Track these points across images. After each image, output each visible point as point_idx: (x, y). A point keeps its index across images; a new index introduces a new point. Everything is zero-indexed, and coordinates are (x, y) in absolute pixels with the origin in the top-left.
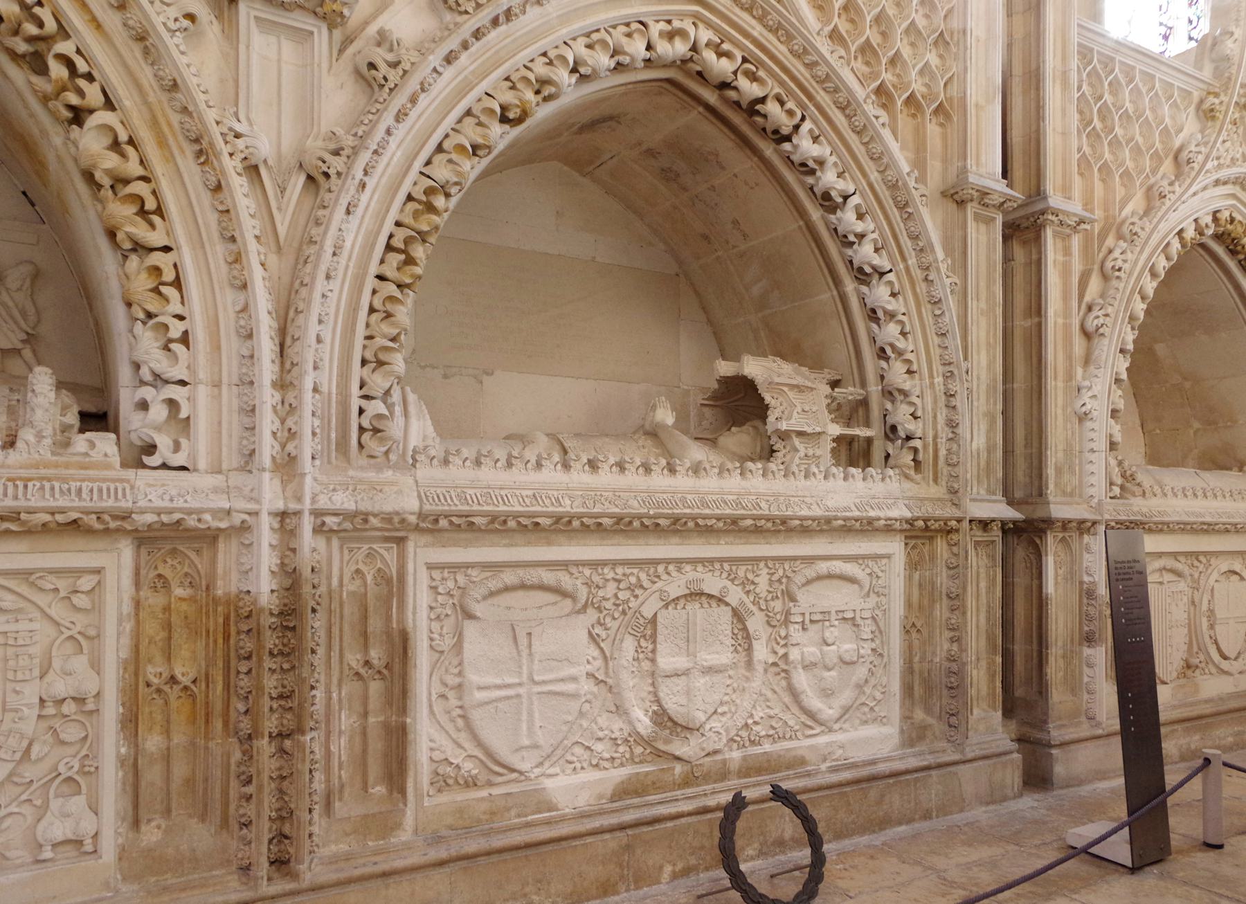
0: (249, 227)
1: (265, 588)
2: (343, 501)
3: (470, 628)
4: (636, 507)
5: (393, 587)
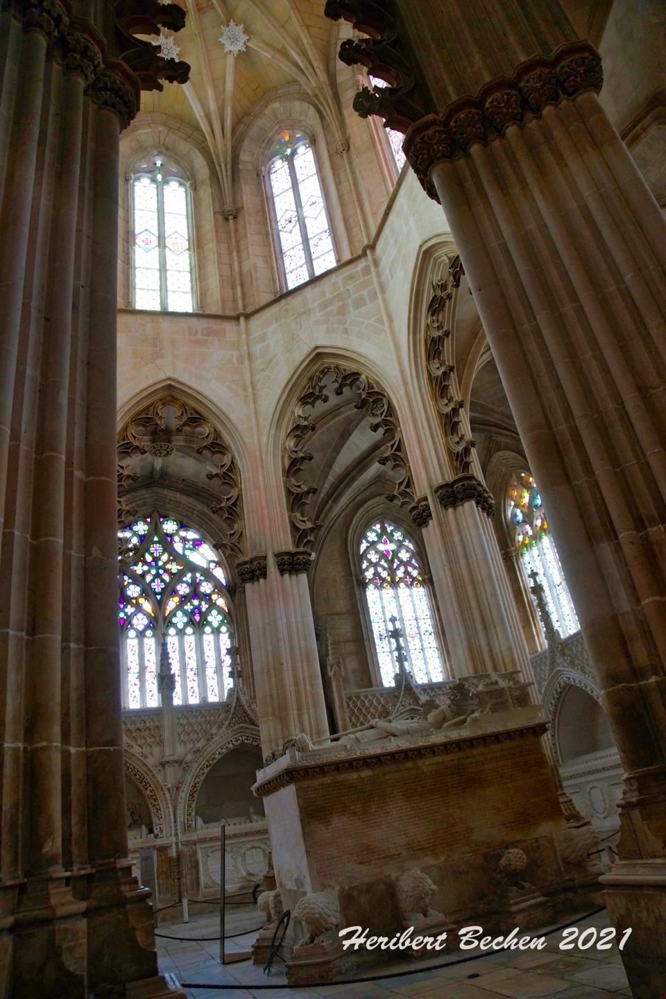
0: (169, 799)
1: (174, 854)
2: (185, 839)
3: (209, 859)
4: (237, 832)
5: (195, 853)
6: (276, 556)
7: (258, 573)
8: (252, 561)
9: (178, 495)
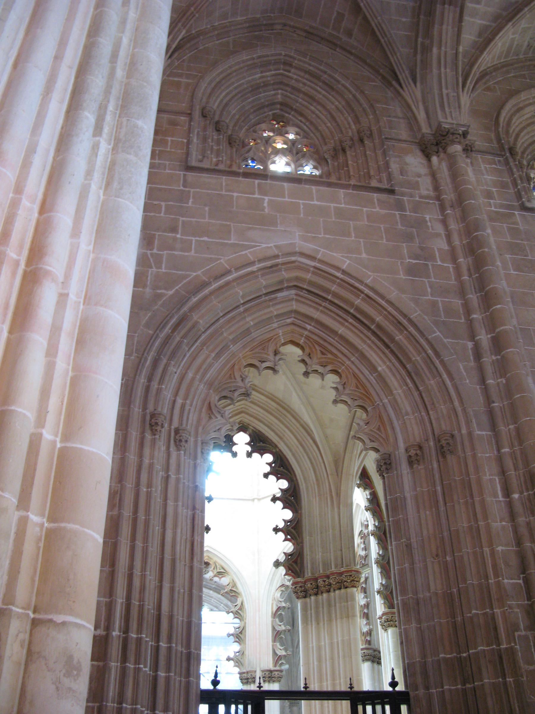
6: (263, 671)
7: (250, 680)
8: (247, 673)
9: (211, 592)
